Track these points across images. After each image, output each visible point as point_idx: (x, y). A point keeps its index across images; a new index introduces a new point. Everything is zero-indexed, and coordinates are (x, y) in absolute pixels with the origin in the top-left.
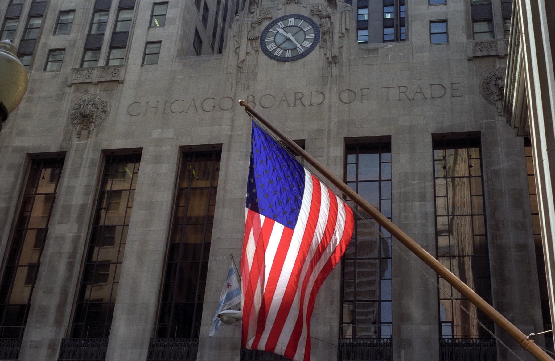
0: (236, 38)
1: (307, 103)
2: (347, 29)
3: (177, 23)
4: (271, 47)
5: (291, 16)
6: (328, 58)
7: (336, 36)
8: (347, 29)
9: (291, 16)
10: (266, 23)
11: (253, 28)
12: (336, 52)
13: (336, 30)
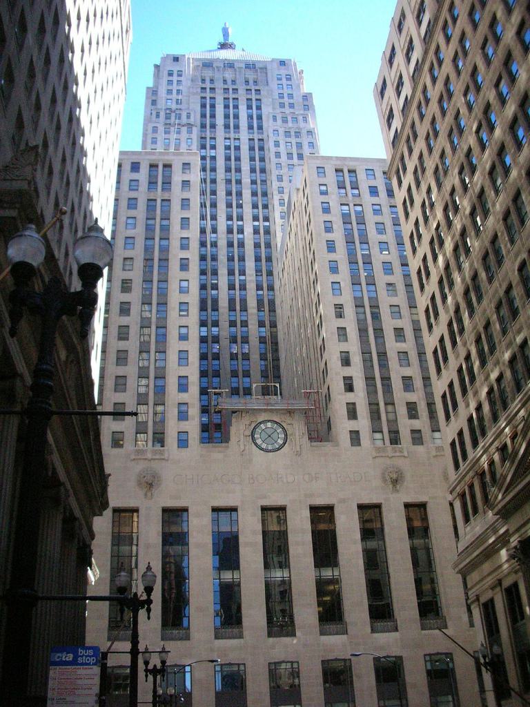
1: (285, 480)
3: (196, 419)
4: (259, 442)
7: (297, 437)
9: (269, 421)
13: (297, 434)
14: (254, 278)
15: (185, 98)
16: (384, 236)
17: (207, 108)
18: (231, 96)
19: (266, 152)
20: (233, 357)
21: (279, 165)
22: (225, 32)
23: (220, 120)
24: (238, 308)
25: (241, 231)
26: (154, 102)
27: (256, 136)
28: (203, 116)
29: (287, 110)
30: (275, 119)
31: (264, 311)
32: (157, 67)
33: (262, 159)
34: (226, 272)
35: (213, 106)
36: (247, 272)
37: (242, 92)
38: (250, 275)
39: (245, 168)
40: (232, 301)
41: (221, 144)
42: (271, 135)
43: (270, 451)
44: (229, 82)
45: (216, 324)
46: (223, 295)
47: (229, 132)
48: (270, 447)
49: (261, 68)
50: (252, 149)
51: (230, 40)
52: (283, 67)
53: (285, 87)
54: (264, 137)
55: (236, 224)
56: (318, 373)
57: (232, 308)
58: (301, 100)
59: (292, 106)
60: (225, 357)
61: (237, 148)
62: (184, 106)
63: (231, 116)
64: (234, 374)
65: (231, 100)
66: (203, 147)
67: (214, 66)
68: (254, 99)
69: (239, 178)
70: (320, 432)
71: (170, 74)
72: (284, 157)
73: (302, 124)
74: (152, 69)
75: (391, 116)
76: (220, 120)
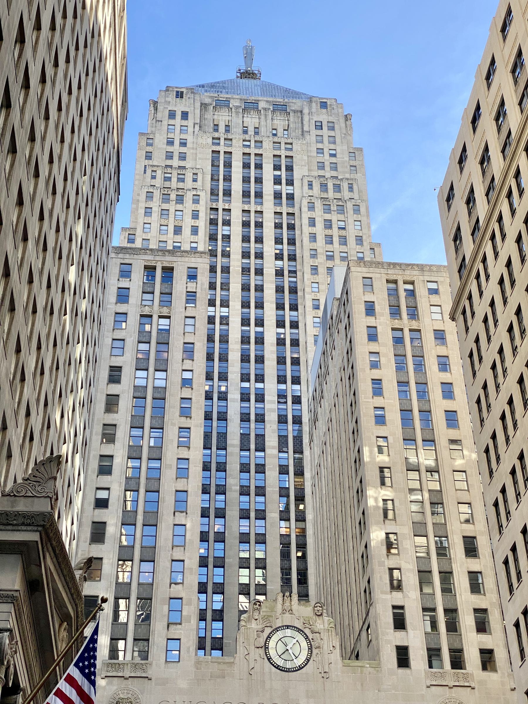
0: (245, 644)
2: (333, 647)
3: (192, 622)
5: (288, 627)
6: (320, 673)
8: (333, 647)
9: (288, 627)
10: (268, 631)
11: (258, 636)
12: (327, 671)
13: (325, 647)
14: (275, 406)
15: (191, 151)
16: (448, 374)
18: (253, 151)
19: (297, 232)
22: (249, 55)
23: (237, 186)
24: (253, 447)
26: (149, 156)
28: (214, 179)
29: (328, 173)
30: (310, 185)
31: (287, 452)
33: (292, 242)
34: (238, 397)
35: (228, 165)
36: (267, 398)
38: (272, 402)
39: (268, 254)
40: (245, 438)
41: (237, 218)
42: (305, 209)
43: (288, 671)
44: (251, 131)
47: (249, 202)
48: (289, 665)
49: (295, 112)
50: (278, 226)
51: (255, 67)
52: (324, 111)
53: (326, 139)
54: (296, 211)
56: (357, 565)
58: (347, 159)
59: (334, 167)
62: (188, 164)
63: (253, 180)
65: (253, 157)
67: (231, 106)
68: (283, 157)
69: (259, 283)
71: (172, 115)
75: (457, 237)
76: (237, 186)
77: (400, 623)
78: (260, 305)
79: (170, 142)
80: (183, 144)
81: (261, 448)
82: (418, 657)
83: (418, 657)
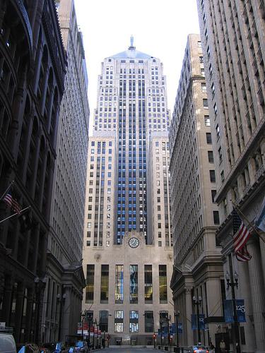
17: (123, 84)
18: (132, 79)
20: (130, 195)
21: (150, 115)
25: (134, 144)
27: (142, 99)
32: (103, 63)
37: (137, 77)
40: (130, 173)
45: (124, 182)
46: (127, 171)
50: (140, 105)
55: (132, 140)
57: (130, 176)
60: (127, 196)
61: (134, 105)
62: (113, 85)
64: (130, 202)
66: (121, 105)
70: (149, 241)
72: (152, 110)
73: (160, 93)
74: (101, 65)
77: (160, 236)
78: (134, 132)
79: (107, 78)
80: (111, 78)
81: (134, 176)
82: (163, 245)
83: (163, 245)
